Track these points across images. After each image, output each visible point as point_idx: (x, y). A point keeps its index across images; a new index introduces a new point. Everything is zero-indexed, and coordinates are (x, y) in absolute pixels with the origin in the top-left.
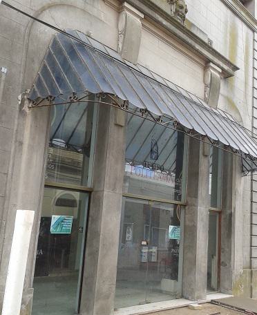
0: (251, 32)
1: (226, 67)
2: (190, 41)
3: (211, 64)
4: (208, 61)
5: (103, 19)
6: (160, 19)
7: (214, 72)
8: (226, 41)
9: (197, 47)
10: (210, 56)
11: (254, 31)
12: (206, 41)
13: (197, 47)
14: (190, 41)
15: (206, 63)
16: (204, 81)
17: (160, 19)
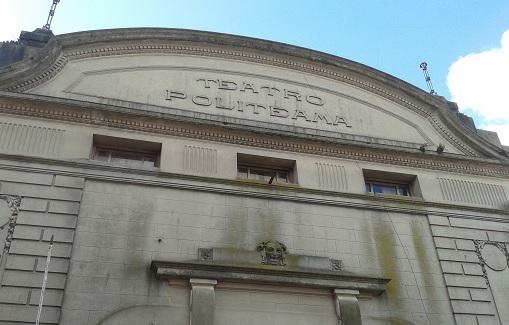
0: (424, 218)
1: (364, 286)
2: (290, 280)
3: (336, 291)
4: (332, 289)
5: (171, 304)
6: (238, 275)
7: (347, 298)
8: (370, 250)
9: (304, 281)
10: (331, 283)
11: (426, 215)
12: (327, 266)
13: (304, 281)
14: (290, 280)
15: (331, 293)
16: (336, 313)
17: (238, 275)
